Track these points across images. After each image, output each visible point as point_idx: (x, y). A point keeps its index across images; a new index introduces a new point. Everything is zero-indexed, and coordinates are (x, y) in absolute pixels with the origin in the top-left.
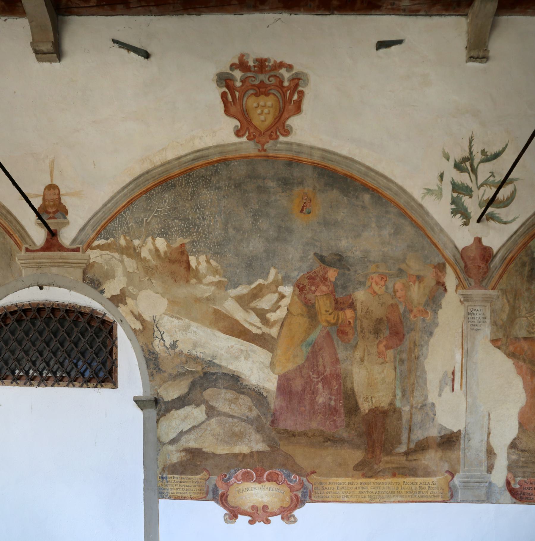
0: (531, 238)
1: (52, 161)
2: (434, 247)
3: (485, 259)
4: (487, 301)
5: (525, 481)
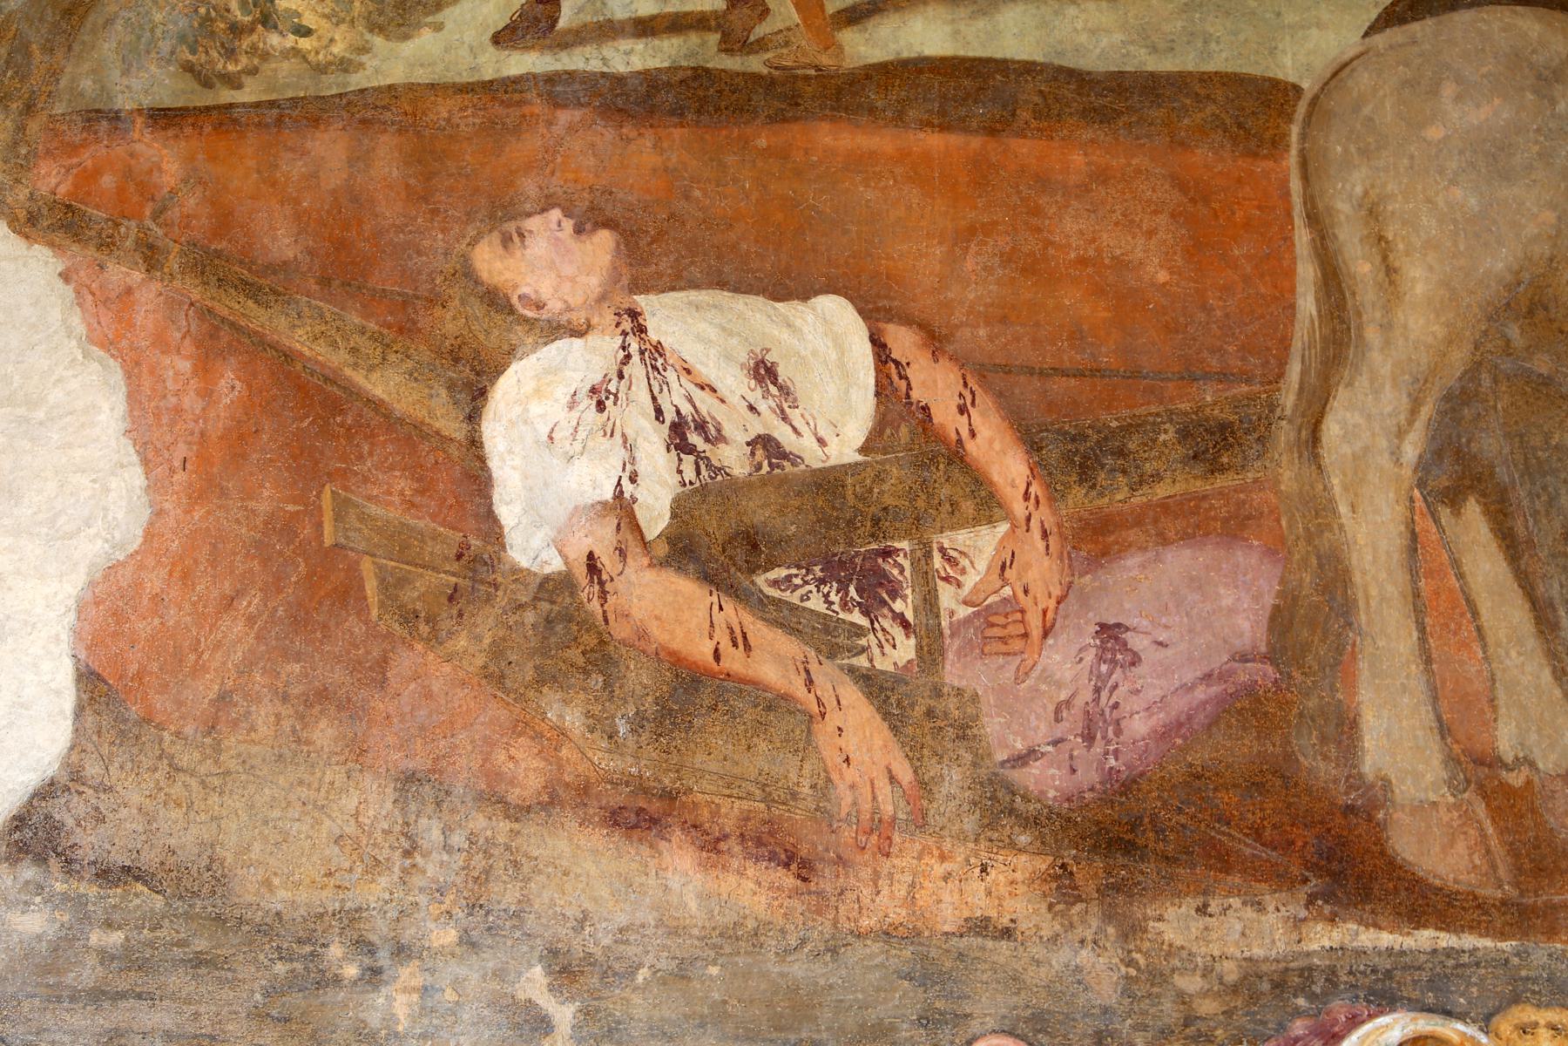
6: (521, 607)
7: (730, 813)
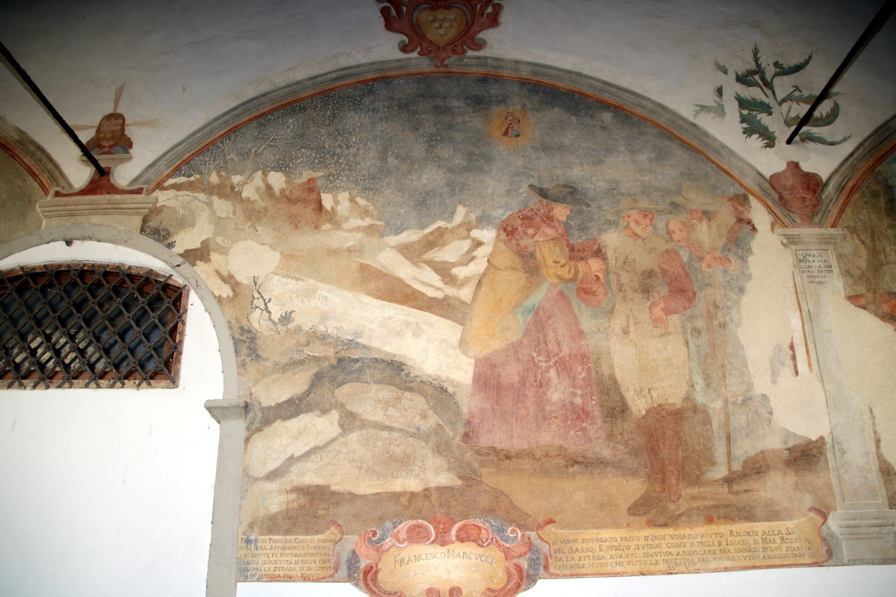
0: (878, 161)
1: (121, 87)
2: (723, 174)
3: (811, 188)
4: (828, 243)
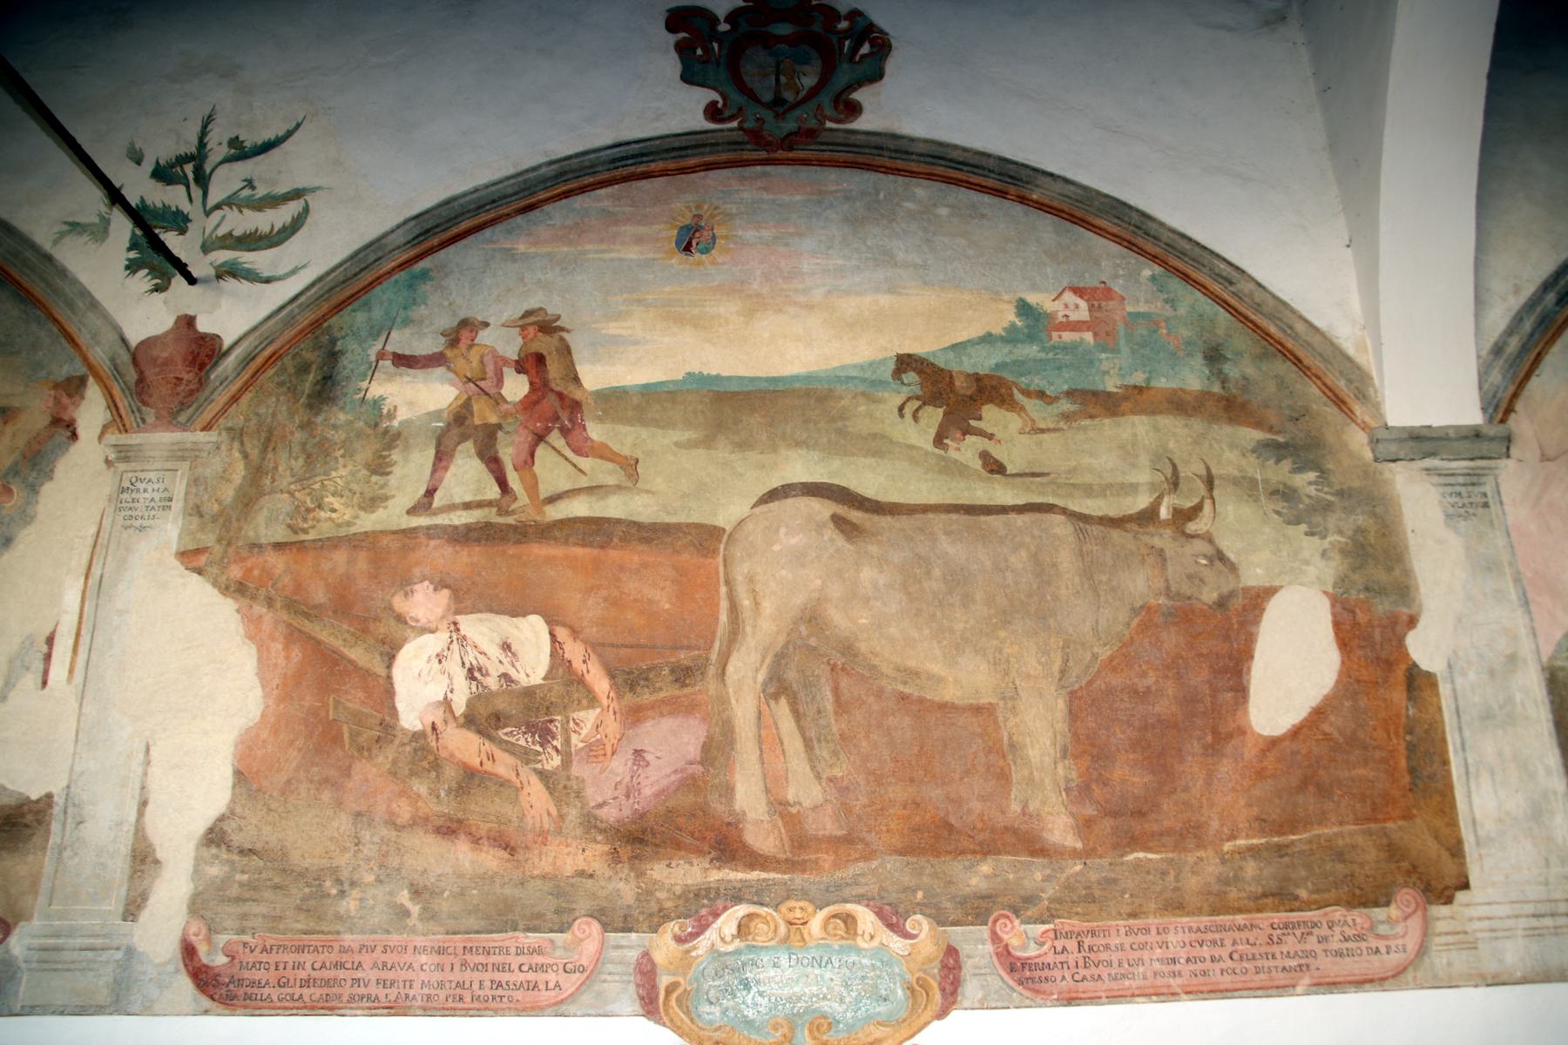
4: (183, 459)
5: (245, 944)
6: (404, 744)
7: (484, 827)
